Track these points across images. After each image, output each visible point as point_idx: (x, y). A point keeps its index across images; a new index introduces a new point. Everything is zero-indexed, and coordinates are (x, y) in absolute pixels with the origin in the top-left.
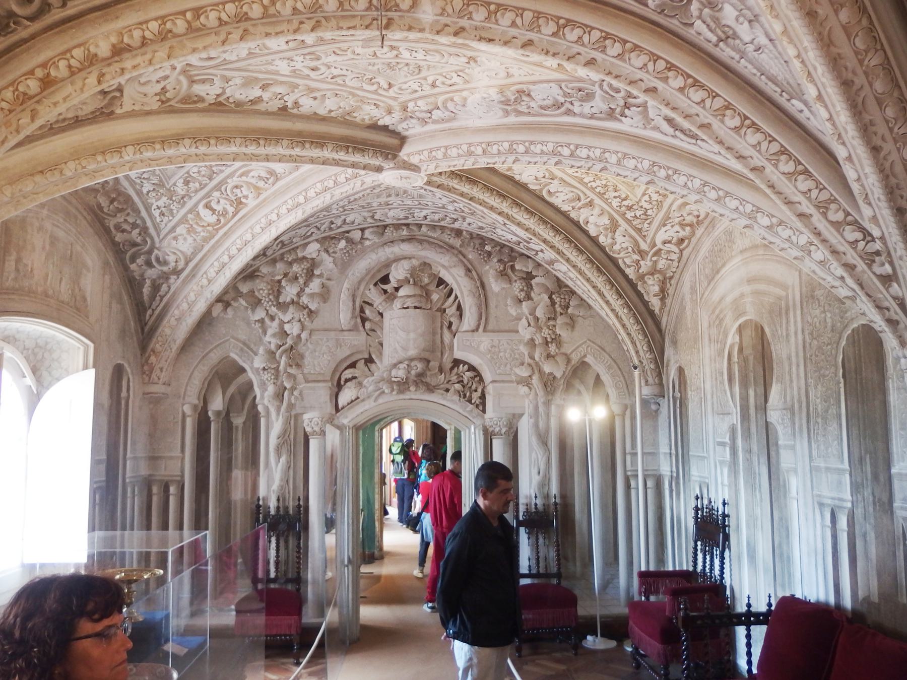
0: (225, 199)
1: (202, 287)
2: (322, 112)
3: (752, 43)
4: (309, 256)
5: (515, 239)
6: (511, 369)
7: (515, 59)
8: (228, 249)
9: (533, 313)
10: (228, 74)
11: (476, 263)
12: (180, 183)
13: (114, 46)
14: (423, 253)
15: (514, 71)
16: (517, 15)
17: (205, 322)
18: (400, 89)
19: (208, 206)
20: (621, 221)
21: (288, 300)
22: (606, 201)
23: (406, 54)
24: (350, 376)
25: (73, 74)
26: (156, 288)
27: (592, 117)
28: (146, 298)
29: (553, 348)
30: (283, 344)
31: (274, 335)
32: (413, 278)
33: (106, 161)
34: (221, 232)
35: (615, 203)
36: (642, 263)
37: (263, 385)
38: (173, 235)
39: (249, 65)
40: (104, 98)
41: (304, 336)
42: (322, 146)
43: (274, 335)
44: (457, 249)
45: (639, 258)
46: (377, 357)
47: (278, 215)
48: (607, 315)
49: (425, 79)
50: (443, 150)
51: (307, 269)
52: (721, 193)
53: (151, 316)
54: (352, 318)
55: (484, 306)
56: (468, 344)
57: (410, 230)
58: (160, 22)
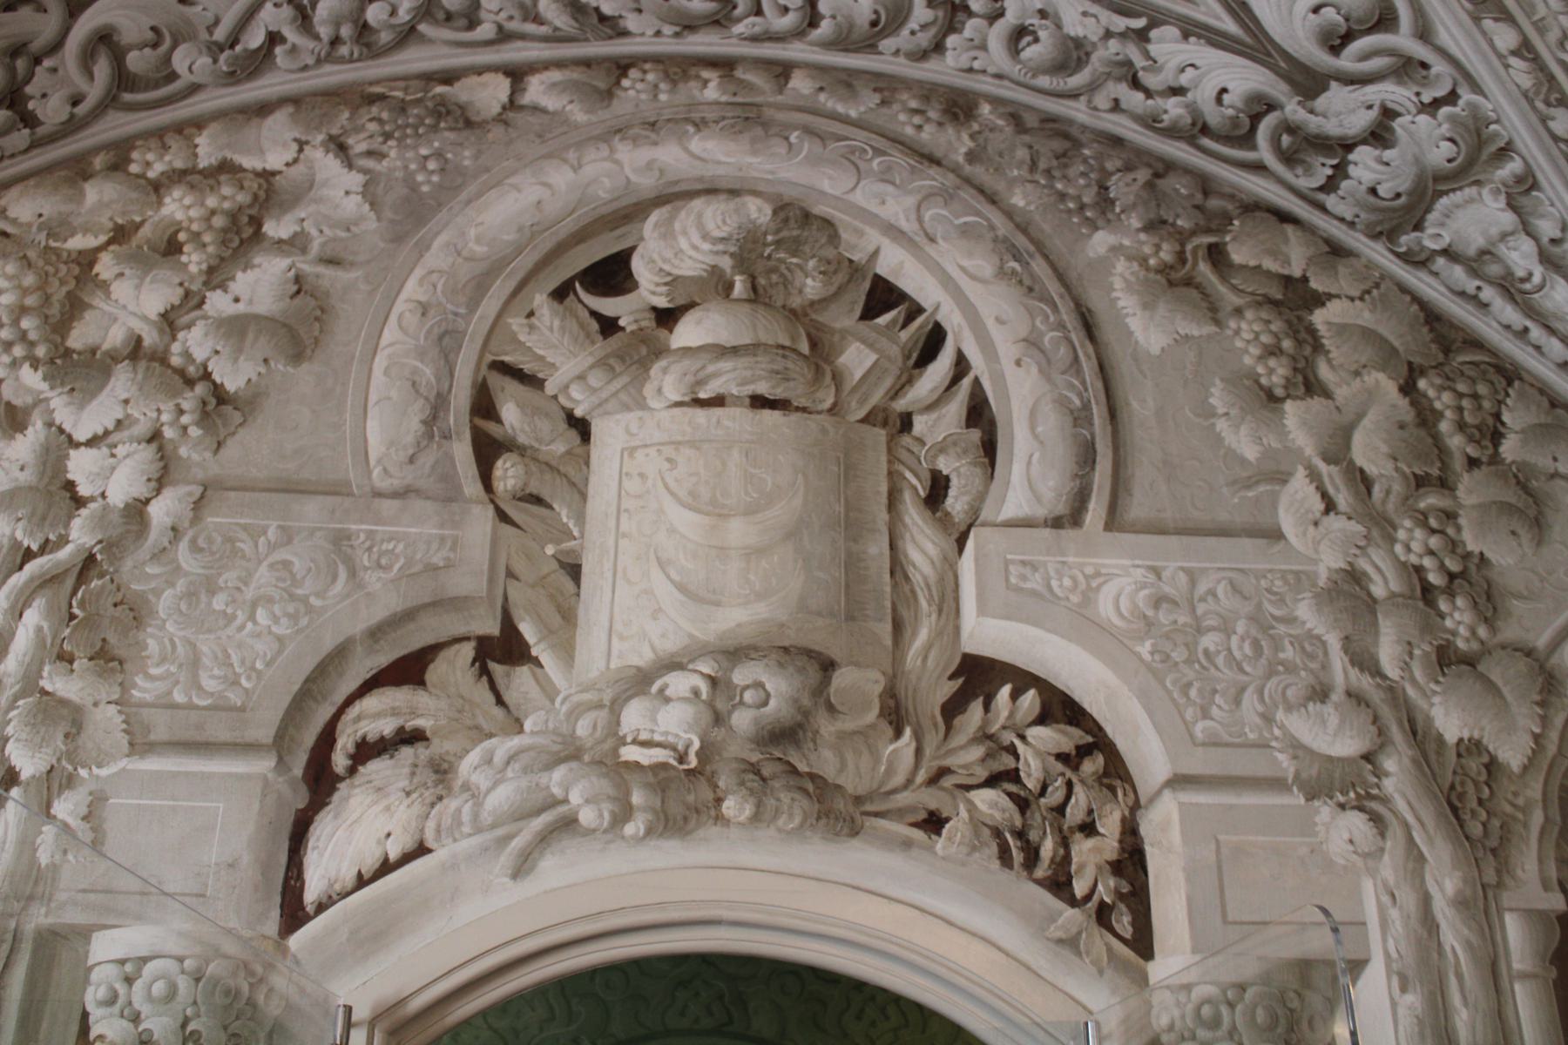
6: (1268, 719)
9: (1337, 450)
11: (1045, 226)
21: (115, 337)
29: (1458, 618)
30: (45, 548)
32: (753, 272)
41: (161, 511)
44: (955, 170)
46: (547, 632)
51: (234, 216)
55: (1098, 413)
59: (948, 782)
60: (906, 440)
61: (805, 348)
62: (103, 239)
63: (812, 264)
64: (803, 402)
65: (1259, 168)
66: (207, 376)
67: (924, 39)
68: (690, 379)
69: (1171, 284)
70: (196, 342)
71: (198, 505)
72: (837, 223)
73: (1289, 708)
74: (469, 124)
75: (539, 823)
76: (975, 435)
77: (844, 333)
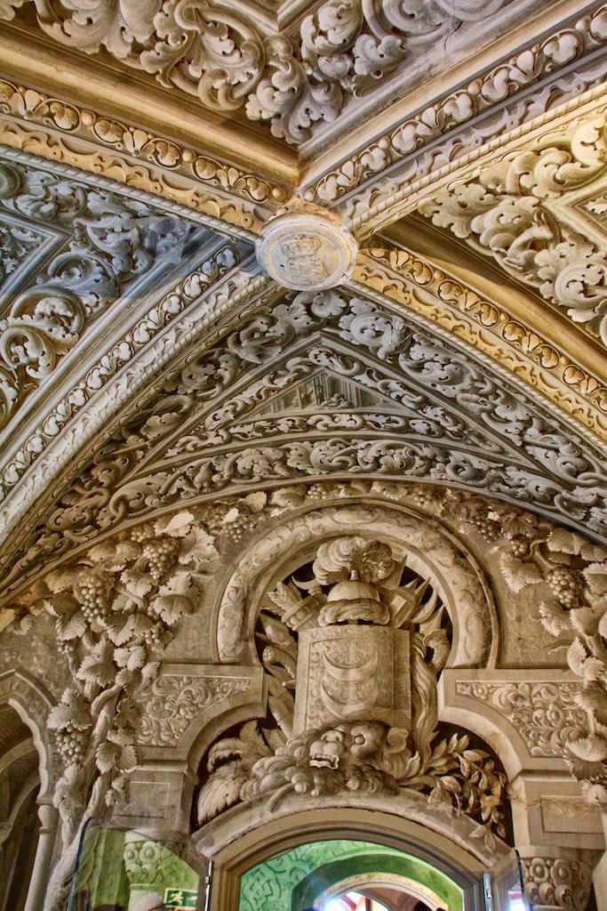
5: (544, 484)
11: (472, 542)
14: (374, 527)
21: (128, 606)
24: (226, 754)
30: (108, 687)
31: (93, 669)
32: (357, 569)
37: (57, 766)
41: (147, 672)
43: (93, 669)
44: (437, 519)
46: (283, 716)
47: (85, 391)
51: (168, 556)
54: (240, 640)
55: (493, 619)
59: (433, 773)
60: (417, 635)
61: (378, 599)
62: (123, 567)
63: (381, 564)
64: (378, 621)
65: (558, 512)
66: (160, 619)
67: (422, 470)
68: (335, 614)
69: (524, 562)
70: (157, 606)
71: (159, 670)
72: (392, 545)
73: (571, 741)
74: (251, 513)
75: (280, 790)
76: (444, 631)
77: (393, 591)
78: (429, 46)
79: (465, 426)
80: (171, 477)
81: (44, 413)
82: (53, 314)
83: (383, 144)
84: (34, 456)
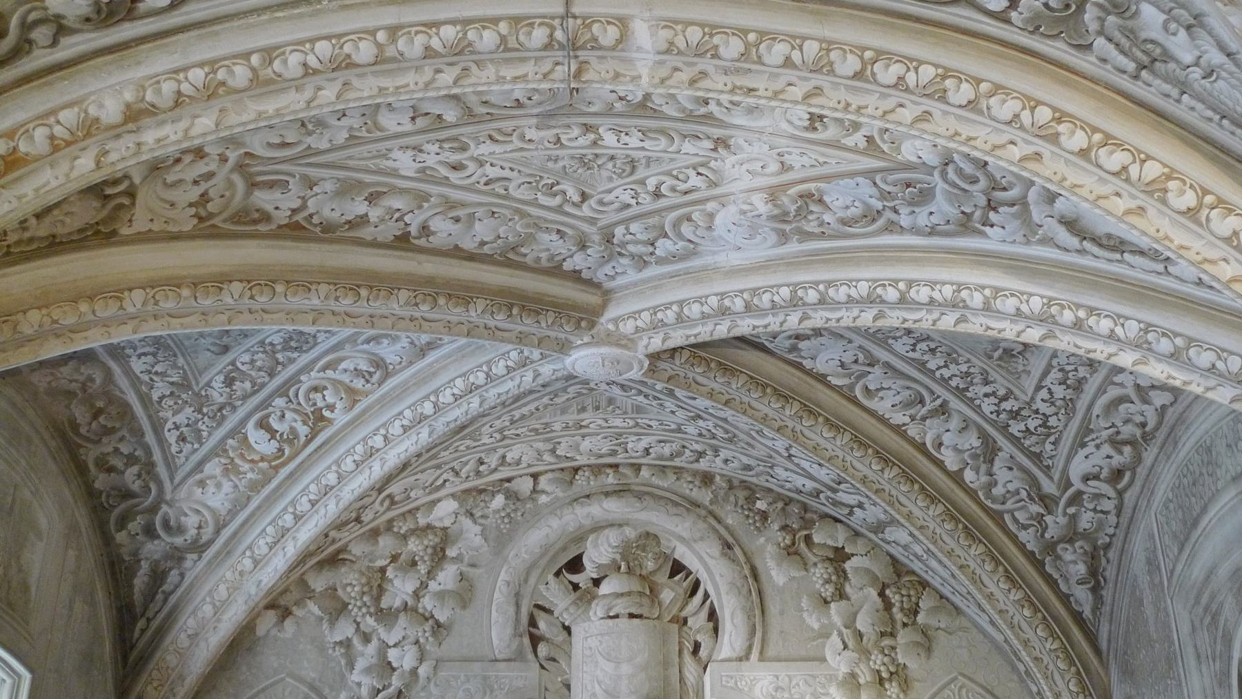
0: (295, 411)
1: (241, 573)
2: (468, 245)
3: (1197, 64)
4: (437, 524)
5: (810, 485)
7: (793, 137)
8: (293, 503)
9: (850, 623)
10: (313, 172)
11: (740, 533)
12: (218, 383)
13: (128, 106)
14: (643, 516)
15: (794, 159)
16: (793, 48)
17: (242, 643)
18: (601, 203)
19: (263, 425)
20: (1001, 441)
21: (397, 603)
22: (970, 402)
23: (609, 139)
25: (56, 149)
26: (158, 576)
27: (933, 232)
28: (137, 597)
31: (368, 671)
32: (627, 562)
33: (94, 312)
34: (284, 472)
35: (988, 406)
36: (1048, 519)
38: (198, 477)
39: (350, 158)
40: (103, 206)
41: (423, 671)
42: (467, 302)
43: (368, 671)
44: (705, 508)
45: (1042, 511)
47: (385, 437)
48: (992, 623)
49: (642, 182)
50: (675, 308)
51: (434, 548)
52: (1179, 341)
53: (143, 631)
55: (758, 612)
56: (732, 684)
57: (618, 477)
58: (207, 69)
60: (685, 628)
66: (432, 616)
70: (427, 603)
72: (659, 534)
74: (518, 500)
76: (711, 624)
78: (714, 253)
79: (735, 436)
80: (439, 472)
81: (342, 449)
82: (356, 369)
83: (675, 308)
84: (328, 489)
